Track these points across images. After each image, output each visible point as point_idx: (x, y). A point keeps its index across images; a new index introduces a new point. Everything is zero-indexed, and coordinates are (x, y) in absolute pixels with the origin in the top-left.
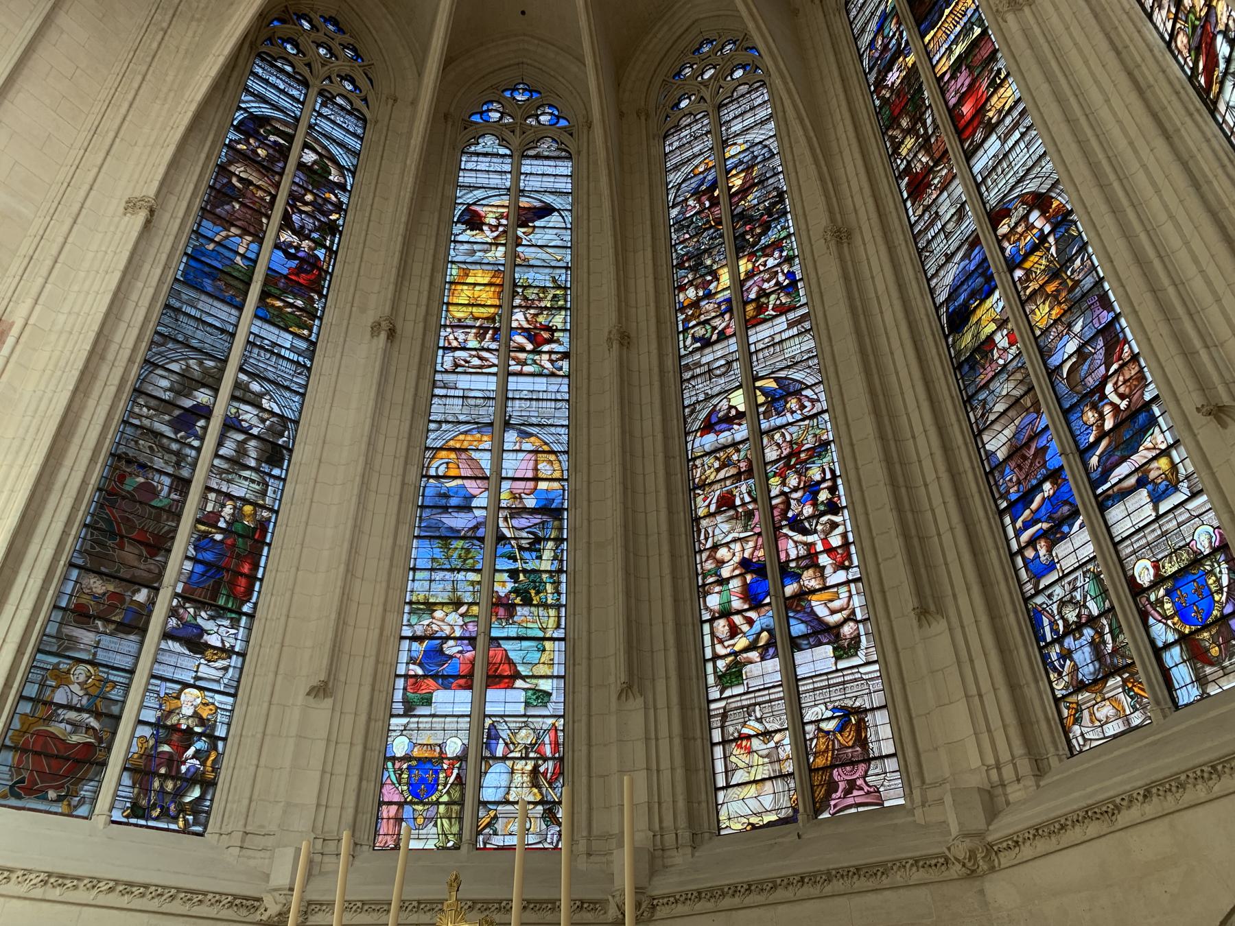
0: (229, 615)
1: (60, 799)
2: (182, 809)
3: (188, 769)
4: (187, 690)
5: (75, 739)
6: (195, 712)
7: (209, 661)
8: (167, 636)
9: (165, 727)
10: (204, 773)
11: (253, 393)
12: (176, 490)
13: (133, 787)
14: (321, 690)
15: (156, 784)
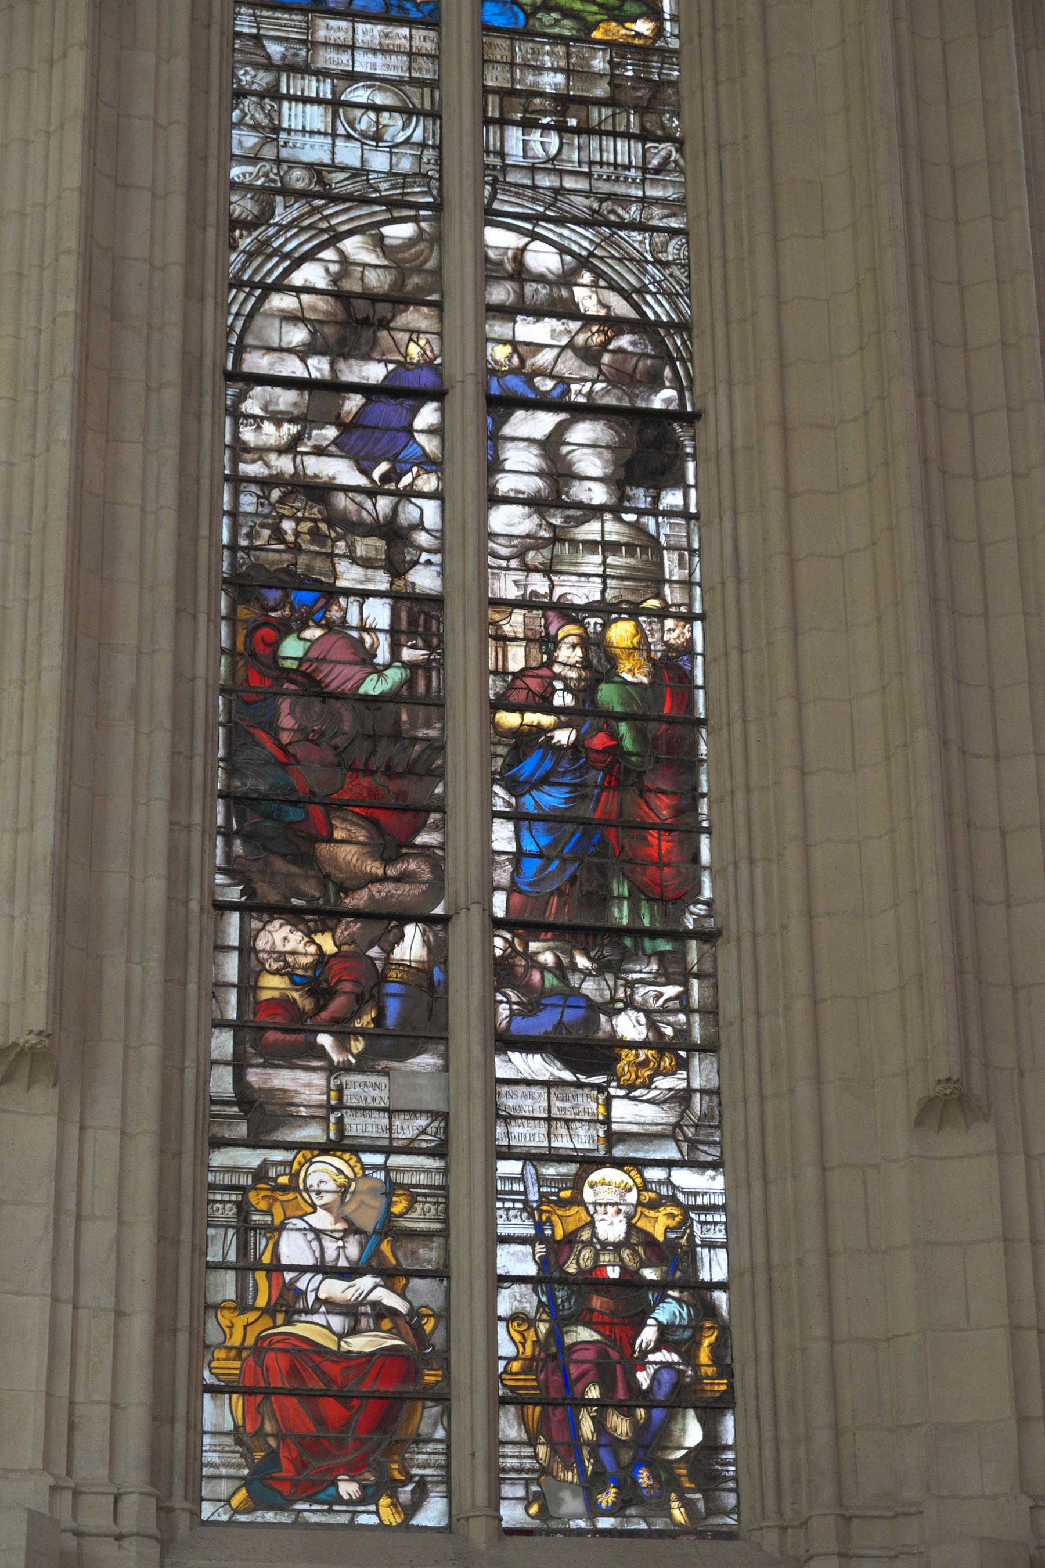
0: (648, 944)
1: (368, 1497)
2: (667, 1481)
3: (653, 1379)
4: (596, 1176)
5: (359, 1344)
6: (631, 1227)
7: (632, 1087)
8: (507, 1042)
9: (566, 1280)
10: (698, 1379)
11: (540, 278)
12: (412, 633)
13: (532, 1443)
14: (950, 1105)
15: (587, 1427)
